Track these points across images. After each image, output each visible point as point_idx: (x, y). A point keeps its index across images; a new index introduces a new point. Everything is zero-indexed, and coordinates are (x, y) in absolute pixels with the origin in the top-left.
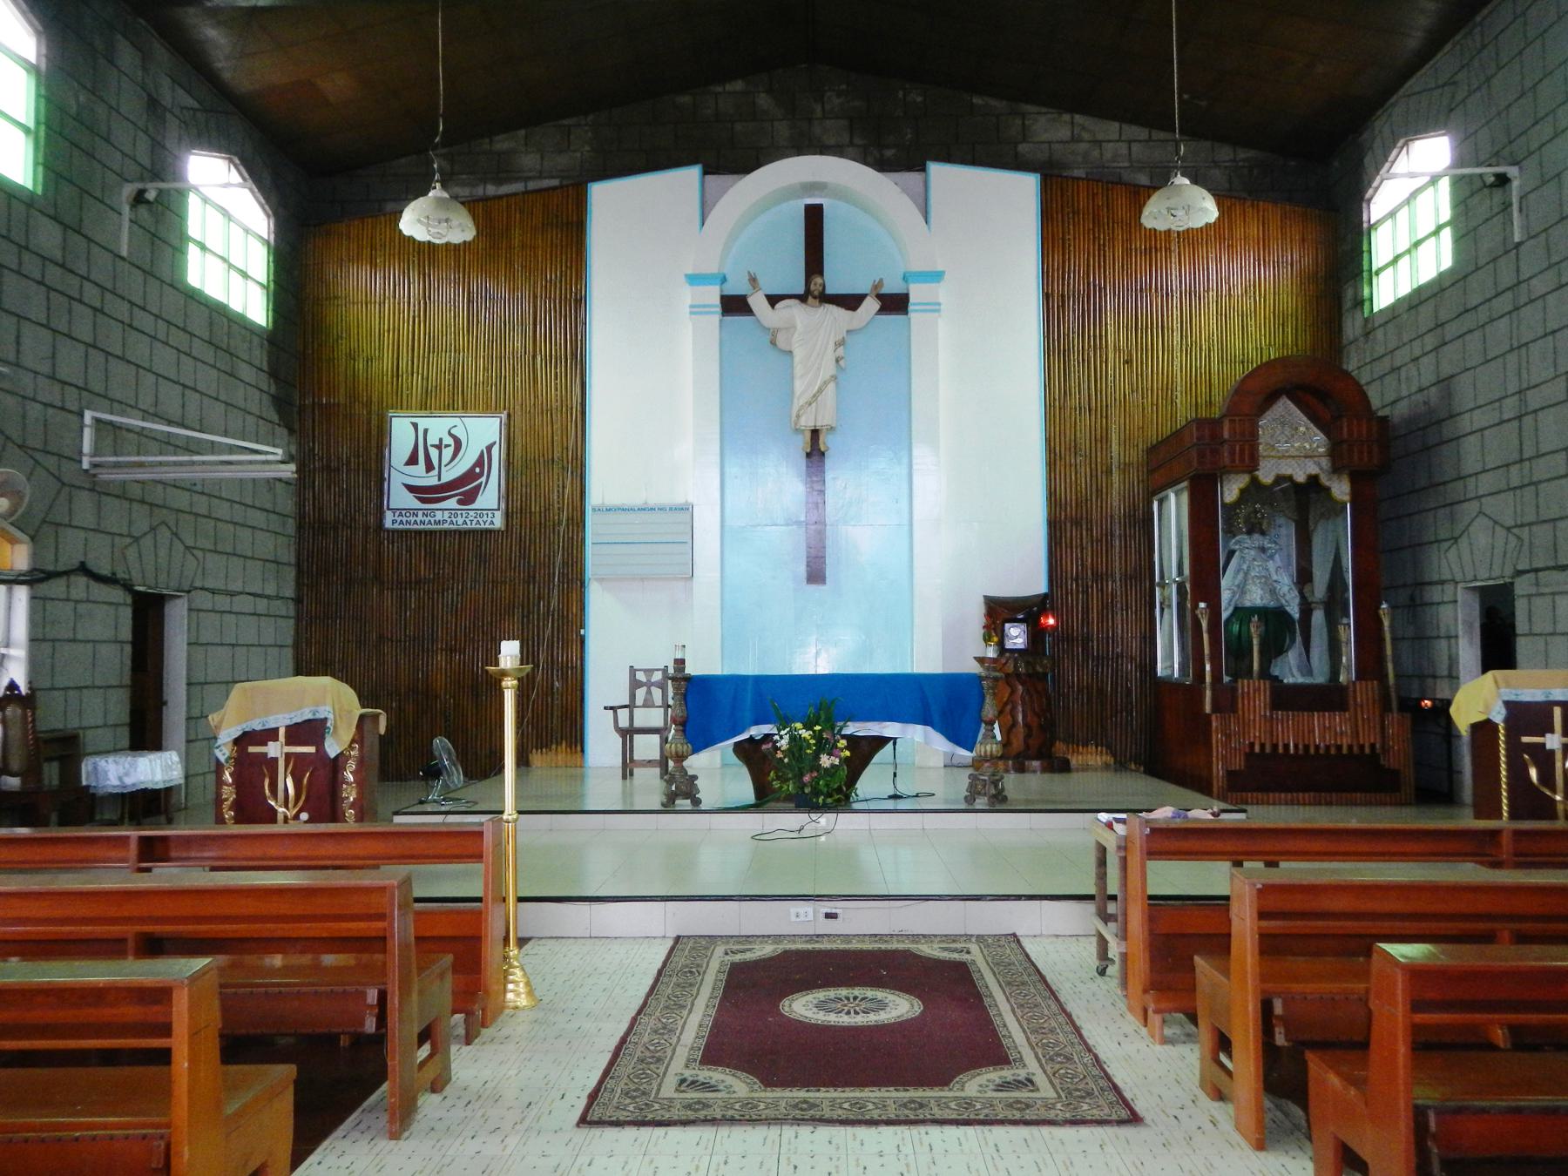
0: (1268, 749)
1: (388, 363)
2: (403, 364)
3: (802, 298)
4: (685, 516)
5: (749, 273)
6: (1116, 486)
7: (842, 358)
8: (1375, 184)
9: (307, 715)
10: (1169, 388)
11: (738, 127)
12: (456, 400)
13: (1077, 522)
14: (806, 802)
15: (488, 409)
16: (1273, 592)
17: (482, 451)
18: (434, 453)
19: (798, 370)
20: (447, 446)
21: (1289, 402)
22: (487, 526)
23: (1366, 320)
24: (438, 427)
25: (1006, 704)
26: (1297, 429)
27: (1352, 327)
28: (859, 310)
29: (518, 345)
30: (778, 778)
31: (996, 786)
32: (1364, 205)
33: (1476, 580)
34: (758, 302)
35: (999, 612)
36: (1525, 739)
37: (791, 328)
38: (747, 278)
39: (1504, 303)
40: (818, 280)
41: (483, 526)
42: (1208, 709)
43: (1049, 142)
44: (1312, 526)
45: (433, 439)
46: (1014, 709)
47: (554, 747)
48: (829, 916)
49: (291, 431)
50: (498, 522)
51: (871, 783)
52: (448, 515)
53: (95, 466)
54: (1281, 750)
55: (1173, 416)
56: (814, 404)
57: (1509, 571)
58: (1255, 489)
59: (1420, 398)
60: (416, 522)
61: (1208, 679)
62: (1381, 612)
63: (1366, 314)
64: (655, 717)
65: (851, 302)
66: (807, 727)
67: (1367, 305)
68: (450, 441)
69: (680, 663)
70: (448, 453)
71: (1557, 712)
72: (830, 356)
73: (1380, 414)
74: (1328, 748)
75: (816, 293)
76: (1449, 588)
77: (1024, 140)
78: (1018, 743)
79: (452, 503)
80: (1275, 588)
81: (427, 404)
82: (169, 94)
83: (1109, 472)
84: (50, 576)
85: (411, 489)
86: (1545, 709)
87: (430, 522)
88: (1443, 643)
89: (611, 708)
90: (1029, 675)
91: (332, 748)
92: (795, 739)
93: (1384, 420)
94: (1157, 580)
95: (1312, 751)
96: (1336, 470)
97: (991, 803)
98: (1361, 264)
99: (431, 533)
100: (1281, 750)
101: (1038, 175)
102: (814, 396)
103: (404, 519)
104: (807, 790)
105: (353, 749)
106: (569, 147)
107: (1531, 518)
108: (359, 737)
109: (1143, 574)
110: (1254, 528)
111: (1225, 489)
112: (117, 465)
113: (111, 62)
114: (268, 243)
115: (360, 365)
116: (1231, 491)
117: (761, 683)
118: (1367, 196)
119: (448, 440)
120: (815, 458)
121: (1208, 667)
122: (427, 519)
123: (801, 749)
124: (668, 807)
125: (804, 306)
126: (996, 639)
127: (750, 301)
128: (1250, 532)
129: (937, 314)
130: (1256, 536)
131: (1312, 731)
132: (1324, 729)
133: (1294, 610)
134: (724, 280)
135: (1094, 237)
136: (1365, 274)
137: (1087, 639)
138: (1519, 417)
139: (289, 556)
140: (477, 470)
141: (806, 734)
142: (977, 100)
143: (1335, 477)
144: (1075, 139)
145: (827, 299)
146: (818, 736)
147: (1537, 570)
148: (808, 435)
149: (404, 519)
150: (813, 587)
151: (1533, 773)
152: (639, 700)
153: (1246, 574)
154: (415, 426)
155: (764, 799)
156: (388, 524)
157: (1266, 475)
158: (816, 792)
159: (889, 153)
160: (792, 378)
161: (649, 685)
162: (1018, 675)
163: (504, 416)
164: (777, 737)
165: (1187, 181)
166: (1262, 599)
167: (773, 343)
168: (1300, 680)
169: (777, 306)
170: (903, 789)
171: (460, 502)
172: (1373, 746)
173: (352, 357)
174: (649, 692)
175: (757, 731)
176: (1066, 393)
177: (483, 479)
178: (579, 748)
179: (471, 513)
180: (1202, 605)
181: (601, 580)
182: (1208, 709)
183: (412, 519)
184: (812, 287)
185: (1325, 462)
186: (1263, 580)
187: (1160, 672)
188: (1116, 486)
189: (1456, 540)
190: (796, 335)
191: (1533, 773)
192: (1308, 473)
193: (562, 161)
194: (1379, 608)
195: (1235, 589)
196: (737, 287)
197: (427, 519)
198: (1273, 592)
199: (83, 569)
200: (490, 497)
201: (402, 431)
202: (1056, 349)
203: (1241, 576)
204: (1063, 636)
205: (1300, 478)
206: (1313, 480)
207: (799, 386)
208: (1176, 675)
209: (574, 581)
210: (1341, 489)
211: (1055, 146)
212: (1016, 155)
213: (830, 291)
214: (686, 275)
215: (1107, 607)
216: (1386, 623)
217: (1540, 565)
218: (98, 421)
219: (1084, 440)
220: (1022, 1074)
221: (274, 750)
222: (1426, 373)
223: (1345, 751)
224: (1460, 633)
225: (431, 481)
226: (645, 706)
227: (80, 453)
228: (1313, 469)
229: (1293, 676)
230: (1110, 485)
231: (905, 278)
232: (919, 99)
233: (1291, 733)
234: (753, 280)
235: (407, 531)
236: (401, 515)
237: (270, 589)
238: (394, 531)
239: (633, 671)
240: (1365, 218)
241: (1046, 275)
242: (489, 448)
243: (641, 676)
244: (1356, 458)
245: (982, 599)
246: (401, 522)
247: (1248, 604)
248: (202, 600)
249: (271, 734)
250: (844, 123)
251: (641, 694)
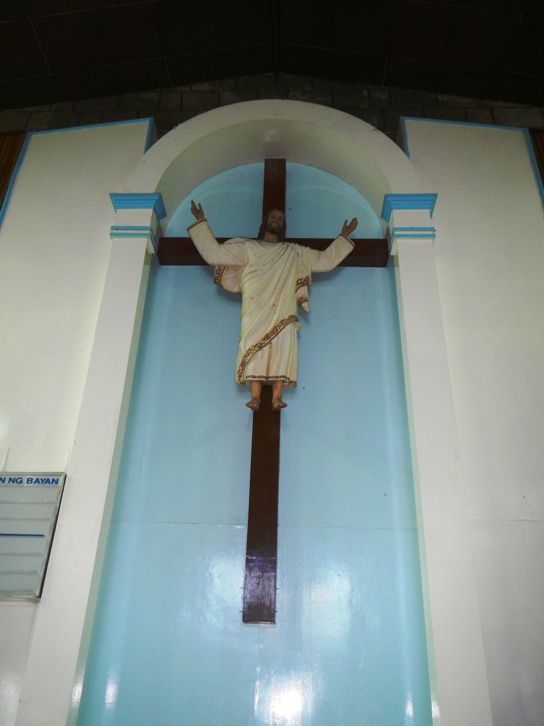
4: (51, 492)
5: (193, 203)
7: (306, 300)
40: (277, 213)
56: (266, 349)
102: (267, 337)
129: (430, 241)
148: (256, 389)
213: (289, 234)
214: (112, 195)
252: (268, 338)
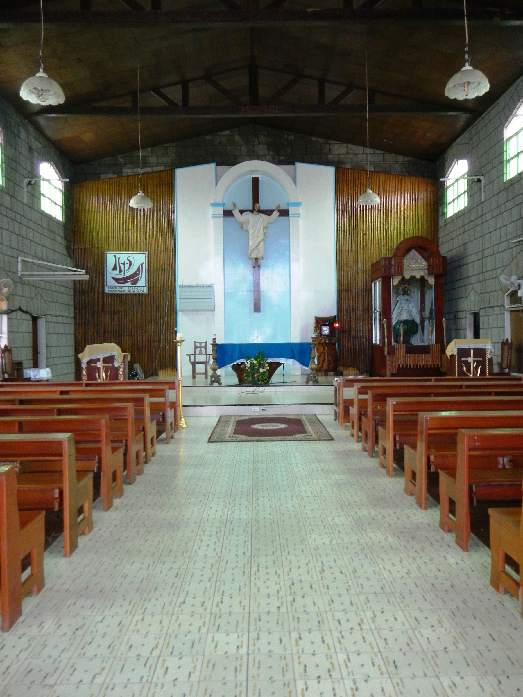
0: (404, 366)
1: (105, 234)
2: (110, 234)
3: (252, 211)
6: (361, 278)
8: (448, 173)
9: (109, 354)
10: (379, 243)
11: (228, 148)
12: (130, 248)
13: (347, 291)
14: (255, 383)
15: (141, 251)
16: (411, 315)
17: (139, 266)
18: (122, 266)
19: (251, 238)
20: (127, 264)
21: (415, 251)
22: (142, 292)
23: (445, 220)
24: (123, 257)
25: (322, 353)
26: (417, 260)
27: (441, 223)
28: (272, 215)
29: (151, 229)
30: (246, 376)
31: (315, 378)
33: (470, 311)
34: (236, 213)
35: (320, 322)
36: (462, 359)
37: (248, 222)
38: (232, 204)
39: (479, 221)
40: (258, 205)
41: (140, 292)
42: (386, 353)
43: (339, 154)
45: (121, 261)
46: (324, 354)
47: (166, 369)
48: (263, 410)
49: (71, 258)
50: (145, 291)
51: (275, 378)
52: (128, 288)
53: (22, 275)
54: (409, 367)
55: (381, 253)
56: (256, 250)
57: (479, 308)
58: (403, 281)
59: (458, 249)
60: (116, 291)
61: (386, 344)
62: (443, 321)
63: (445, 217)
64: (202, 358)
65: (269, 213)
66: (256, 360)
67: (445, 215)
68: (128, 262)
69: (214, 340)
70: (127, 266)
71: (472, 351)
72: (262, 232)
73: (443, 255)
74: (423, 366)
75: (257, 210)
76: (464, 313)
77: (330, 153)
78: (325, 366)
79: (129, 284)
80: (411, 313)
81: (119, 249)
82: (35, 145)
83: (358, 273)
84: (12, 311)
85: (114, 279)
86: (469, 350)
87: (121, 291)
88: (462, 331)
89: (189, 355)
90: (329, 343)
91: (116, 365)
92: (252, 364)
93: (445, 258)
94: (373, 310)
95: (419, 367)
96: (430, 274)
97: (314, 383)
98: (444, 201)
99: (122, 294)
100: (409, 367)
101: (335, 167)
102: (256, 246)
103: (112, 290)
104: (256, 379)
105: (122, 365)
106: (167, 154)
107: (484, 291)
108: (124, 362)
109: (368, 309)
110: (405, 293)
111: (393, 281)
112: (30, 275)
113: (19, 137)
114: (61, 191)
115: (95, 234)
116: (395, 281)
117: (241, 347)
119: (127, 262)
120: (257, 268)
121: (386, 340)
122: (120, 290)
123: (253, 366)
124: (211, 385)
125: (252, 214)
126: (318, 331)
127: (234, 212)
128: (403, 295)
130: (406, 296)
131: (418, 360)
132: (422, 359)
133: (418, 321)
134: (224, 205)
136: (445, 204)
137: (350, 331)
138: (482, 258)
139: (72, 303)
140: (138, 272)
141: (255, 362)
142: (314, 139)
143: (430, 276)
144: (348, 153)
145: (261, 211)
146: (259, 362)
147: (485, 308)
149: (112, 290)
150: (256, 314)
151: (465, 369)
152: (197, 353)
154: (115, 256)
155: (242, 382)
156: (106, 291)
157: (407, 276)
158: (258, 380)
159: (282, 158)
160: (249, 240)
161: (201, 347)
162: (326, 343)
163: (147, 253)
164: (246, 363)
165: (371, 191)
166: (407, 317)
167: (242, 227)
168: (421, 344)
169: (243, 214)
170: (286, 380)
171: (132, 284)
172: (438, 365)
173: (91, 231)
174: (201, 350)
175: (239, 361)
176: (344, 245)
177: (140, 276)
178: (175, 369)
179: (136, 287)
180: (385, 320)
181: (182, 311)
182: (386, 353)
183: (115, 289)
184: (255, 208)
185: (426, 271)
187: (374, 342)
188: (361, 278)
189: (467, 297)
190: (250, 225)
191: (465, 369)
193: (164, 160)
194: (442, 320)
196: (229, 207)
197: (120, 290)
198: (411, 315)
199: (20, 309)
200: (142, 282)
201: (110, 258)
202: (340, 229)
203: (400, 310)
204: (341, 330)
205: (418, 277)
206: (422, 278)
207: (251, 243)
208: (378, 343)
209: (172, 312)
210: (431, 281)
211: (342, 156)
212: (327, 159)
213: (261, 209)
215: (357, 320)
216: (444, 325)
217: (486, 306)
218: (22, 260)
219: (350, 262)
220: (309, 434)
221: (100, 365)
222: (459, 242)
223: (429, 367)
224: (467, 328)
225: (121, 276)
226: (199, 354)
227: (18, 271)
228: (422, 274)
229: (418, 343)
230: (358, 278)
231: (288, 205)
232: (293, 138)
233: (411, 361)
234: (234, 205)
235: (113, 294)
236: (111, 288)
237: (67, 315)
238: (108, 294)
239: (195, 343)
241: (337, 203)
242: (142, 265)
243: (198, 345)
244: (435, 270)
245: (314, 318)
246: (111, 291)
248: (49, 318)
249: (98, 360)
250: (266, 147)
251: (198, 350)
252: (257, 246)
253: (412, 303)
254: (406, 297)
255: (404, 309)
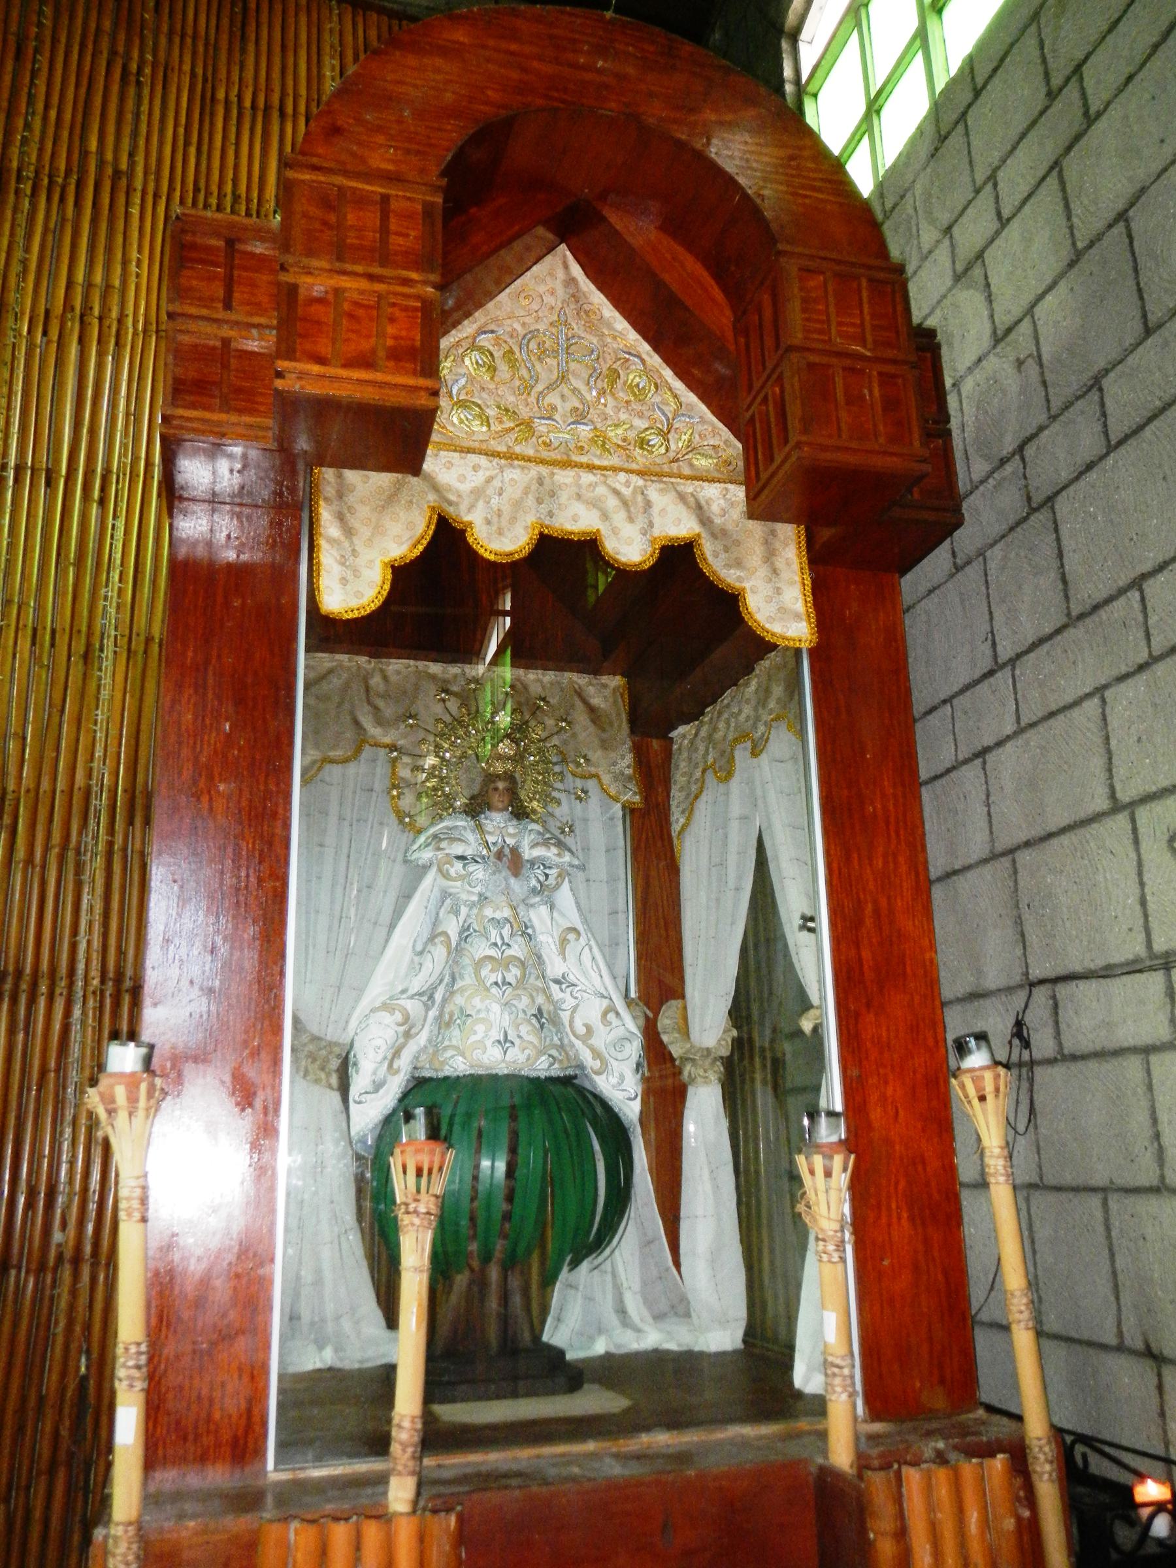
32: (785, 45)
44: (677, 820)
80: (557, 1006)
118: (791, 18)
135: (113, 53)
153: (456, 953)
186: (513, 974)
192: (656, 532)
195: (413, 1007)
240: (788, 72)
247: (458, 1066)
253: (564, 895)
254: (497, 822)
255: (480, 948)
